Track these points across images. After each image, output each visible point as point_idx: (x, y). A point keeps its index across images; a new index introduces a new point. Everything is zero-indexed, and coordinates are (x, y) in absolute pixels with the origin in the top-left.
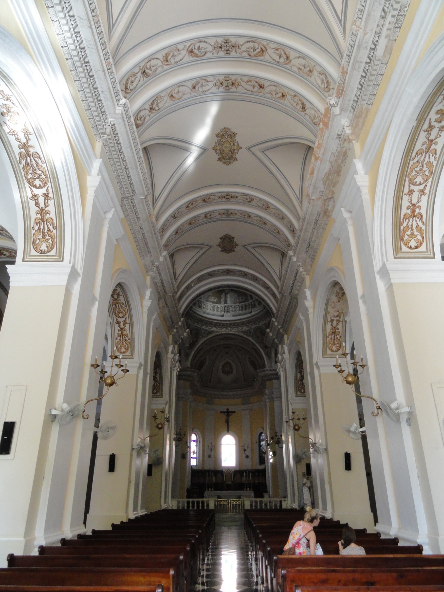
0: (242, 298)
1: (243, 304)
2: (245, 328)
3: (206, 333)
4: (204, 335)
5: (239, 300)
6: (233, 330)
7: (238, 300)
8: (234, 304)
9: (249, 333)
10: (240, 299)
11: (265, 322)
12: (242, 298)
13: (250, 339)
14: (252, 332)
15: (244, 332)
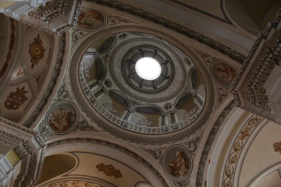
0: (88, 73)
1: (83, 77)
2: (69, 88)
3: (79, 35)
4: (79, 32)
5: (87, 69)
6: (68, 72)
7: (86, 68)
8: (83, 64)
9: (63, 95)
10: (87, 72)
11: (88, 119)
12: (88, 73)
13: (55, 97)
14: (66, 99)
15: (64, 86)
